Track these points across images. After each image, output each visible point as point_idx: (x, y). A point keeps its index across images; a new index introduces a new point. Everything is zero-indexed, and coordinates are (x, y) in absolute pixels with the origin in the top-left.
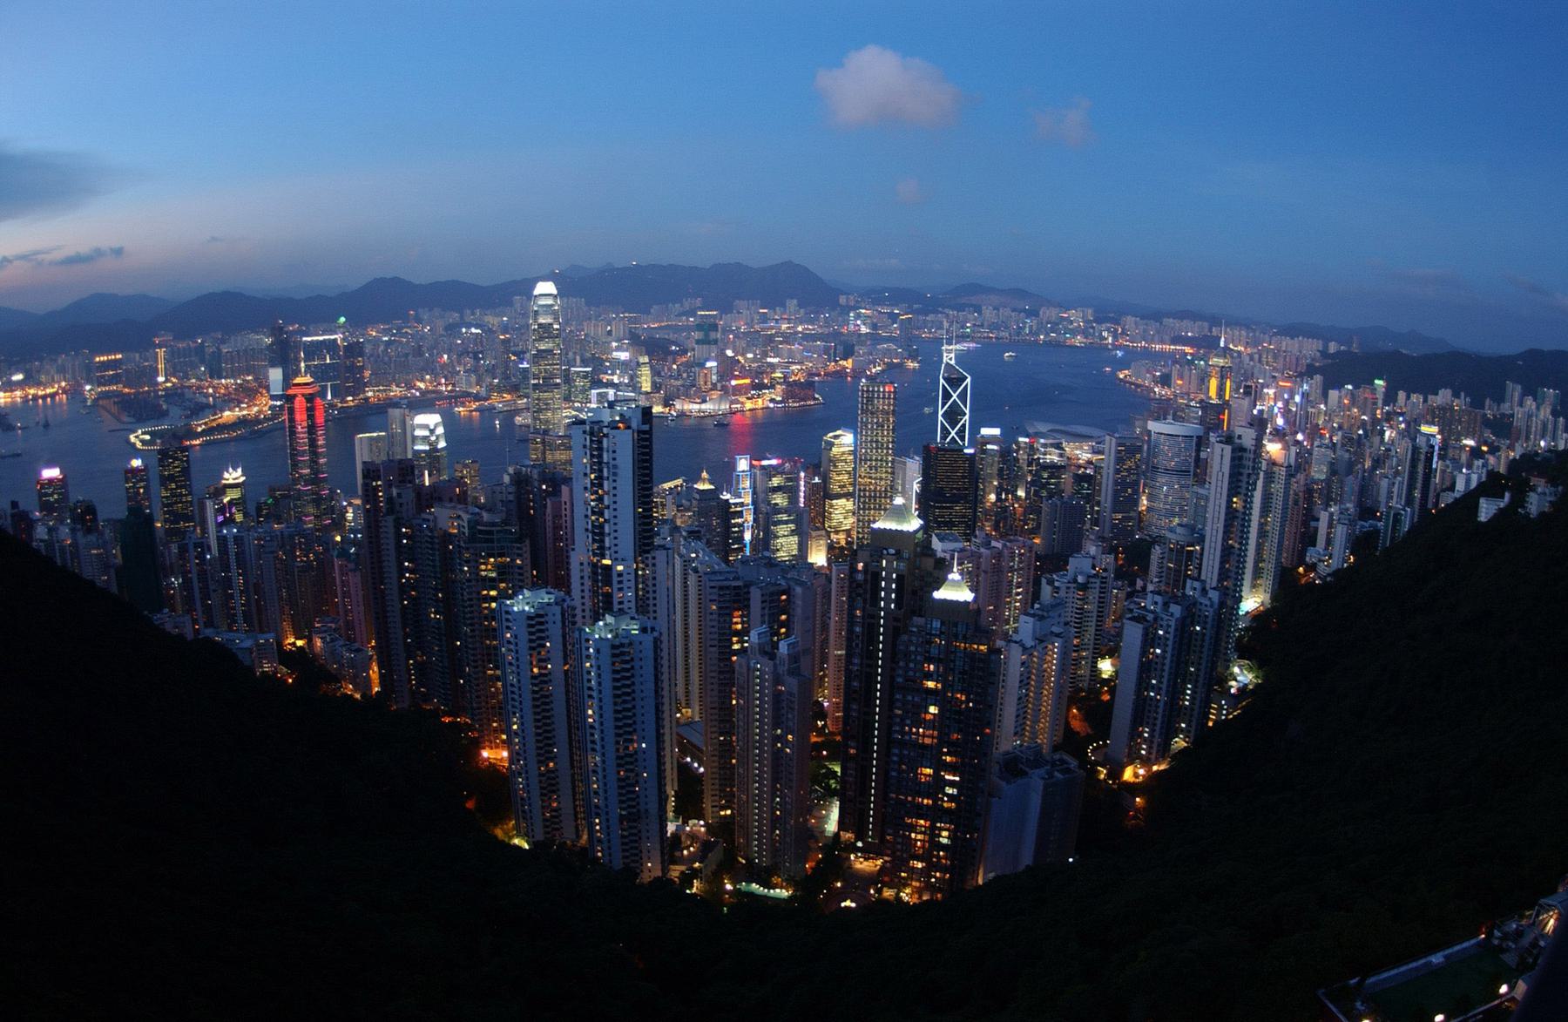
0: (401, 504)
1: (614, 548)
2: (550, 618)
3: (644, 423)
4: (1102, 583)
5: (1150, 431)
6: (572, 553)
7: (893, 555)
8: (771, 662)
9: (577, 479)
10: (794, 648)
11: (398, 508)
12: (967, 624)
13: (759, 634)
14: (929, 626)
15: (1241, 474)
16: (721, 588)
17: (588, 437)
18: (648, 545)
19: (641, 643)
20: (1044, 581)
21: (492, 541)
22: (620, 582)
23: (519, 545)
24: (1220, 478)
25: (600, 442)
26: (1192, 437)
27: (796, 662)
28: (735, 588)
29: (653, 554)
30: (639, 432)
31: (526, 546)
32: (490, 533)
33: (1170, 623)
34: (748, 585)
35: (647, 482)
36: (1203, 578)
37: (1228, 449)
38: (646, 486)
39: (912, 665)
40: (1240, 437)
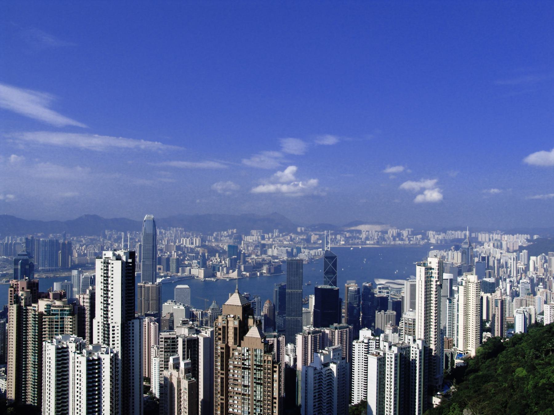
2: (70, 350)
6: (94, 320)
7: (233, 317)
8: (177, 372)
12: (261, 350)
15: (431, 281)
16: (165, 338)
17: (103, 265)
18: (131, 316)
19: (104, 359)
23: (71, 317)
24: (420, 283)
25: (107, 267)
26: (448, 279)
28: (174, 338)
29: (133, 321)
33: (392, 356)
35: (131, 286)
37: (423, 268)
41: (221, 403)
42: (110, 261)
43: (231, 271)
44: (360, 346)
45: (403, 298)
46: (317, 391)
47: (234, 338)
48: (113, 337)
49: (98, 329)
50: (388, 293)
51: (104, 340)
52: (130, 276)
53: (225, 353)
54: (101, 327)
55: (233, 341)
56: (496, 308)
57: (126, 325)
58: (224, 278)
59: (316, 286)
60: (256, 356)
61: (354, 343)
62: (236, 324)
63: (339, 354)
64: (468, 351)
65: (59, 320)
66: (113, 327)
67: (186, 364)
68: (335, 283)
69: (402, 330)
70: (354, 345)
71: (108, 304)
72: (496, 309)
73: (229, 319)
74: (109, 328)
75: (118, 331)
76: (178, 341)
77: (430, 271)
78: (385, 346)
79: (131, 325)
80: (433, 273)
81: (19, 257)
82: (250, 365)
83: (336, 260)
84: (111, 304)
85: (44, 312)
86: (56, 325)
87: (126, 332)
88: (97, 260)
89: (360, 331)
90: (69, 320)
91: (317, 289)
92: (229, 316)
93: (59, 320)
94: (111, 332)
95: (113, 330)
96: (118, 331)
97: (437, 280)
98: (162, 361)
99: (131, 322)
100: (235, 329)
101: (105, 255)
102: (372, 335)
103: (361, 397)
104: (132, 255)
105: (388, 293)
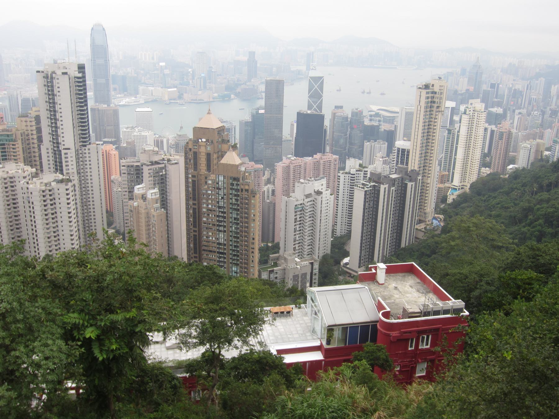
2: (16, 179)
4: (364, 174)
7: (205, 142)
10: (155, 195)
13: (138, 189)
14: (217, 179)
15: (433, 107)
16: (128, 166)
18: (85, 142)
25: (52, 82)
26: (449, 108)
27: (157, 203)
29: (88, 147)
30: (75, 77)
31: (18, 144)
38: (81, 108)
39: (210, 202)
41: (194, 235)
42: (54, 75)
43: (200, 92)
44: (345, 178)
45: (396, 127)
46: (298, 223)
47: (207, 165)
50: (379, 121)
51: (57, 169)
52: (81, 94)
53: (197, 182)
54: (51, 155)
55: (205, 168)
56: (500, 141)
57: (80, 152)
58: (192, 100)
59: (298, 111)
61: (339, 174)
62: (209, 149)
63: (322, 185)
64: (464, 187)
66: (66, 154)
67: (154, 194)
68: (320, 107)
69: (394, 161)
70: (339, 176)
72: (500, 143)
73: (201, 144)
74: (60, 155)
76: (142, 169)
77: (433, 95)
79: (87, 151)
80: (435, 97)
82: (225, 195)
83: (322, 83)
84: (61, 127)
87: (81, 159)
89: (347, 161)
90: (11, 146)
91: (299, 114)
92: (200, 140)
94: (64, 160)
97: (438, 105)
98: (126, 191)
99: (87, 148)
100: (208, 155)
102: (360, 165)
103: (344, 231)
104: (81, 68)
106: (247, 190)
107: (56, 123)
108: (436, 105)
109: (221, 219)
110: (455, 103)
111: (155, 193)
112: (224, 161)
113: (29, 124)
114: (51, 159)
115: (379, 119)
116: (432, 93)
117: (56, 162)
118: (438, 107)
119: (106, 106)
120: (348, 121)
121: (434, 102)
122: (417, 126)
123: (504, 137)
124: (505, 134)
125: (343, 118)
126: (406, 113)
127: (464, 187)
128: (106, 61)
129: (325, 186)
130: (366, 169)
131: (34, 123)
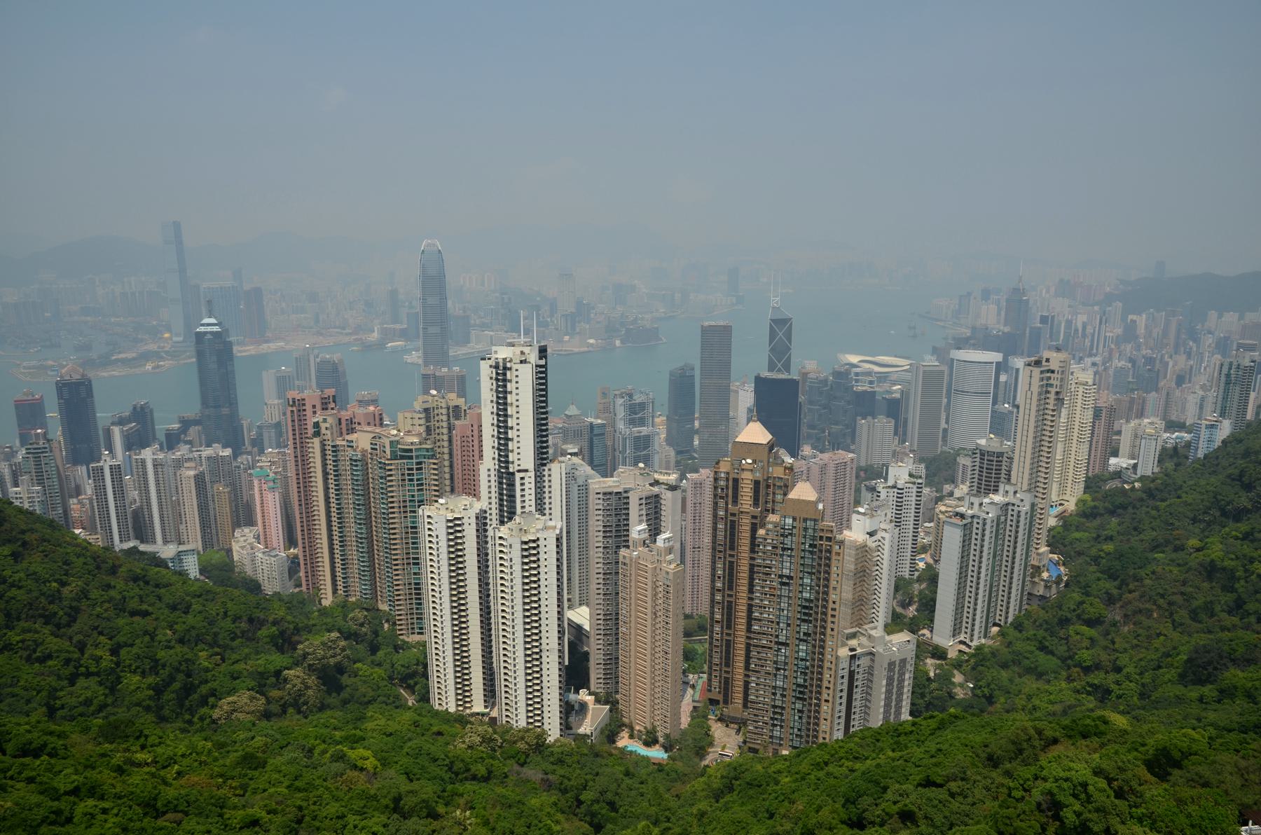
0: (327, 428)
1: (519, 462)
3: (541, 358)
5: (952, 360)
6: (481, 467)
9: (485, 406)
11: (323, 431)
15: (1048, 392)
16: (605, 494)
18: (545, 459)
20: (863, 489)
21: (411, 458)
22: (523, 490)
25: (505, 374)
32: (411, 450)
34: (626, 492)
36: (1013, 480)
40: (1048, 360)
42: (508, 365)
43: (567, 338)
48: (523, 496)
49: (489, 481)
50: (871, 382)
54: (493, 478)
60: (806, 529)
65: (415, 467)
66: (522, 478)
68: (787, 367)
71: (507, 439)
75: (529, 486)
77: (1049, 375)
78: (972, 504)
79: (546, 473)
81: (202, 329)
85: (370, 451)
86: (409, 475)
88: (482, 362)
92: (744, 462)
93: (415, 467)
94: (518, 487)
95: (522, 484)
96: (529, 486)
99: (546, 468)
100: (757, 483)
101: (496, 352)
102: (911, 475)
105: (871, 382)
106: (829, 539)
107: (506, 433)
108: (1053, 390)
109: (785, 580)
110: (1001, 355)
111: (668, 539)
112: (792, 495)
113: (417, 422)
114: (493, 484)
115: (871, 379)
116: (1048, 371)
117: (501, 489)
118: (1057, 393)
119: (445, 370)
120: (826, 385)
121: (1051, 385)
122: (1026, 422)
123: (1104, 415)
124: (1104, 410)
125: (821, 382)
126: (924, 372)
127: (1066, 503)
128: (443, 299)
129: (889, 515)
130: (920, 481)
131: (422, 422)
